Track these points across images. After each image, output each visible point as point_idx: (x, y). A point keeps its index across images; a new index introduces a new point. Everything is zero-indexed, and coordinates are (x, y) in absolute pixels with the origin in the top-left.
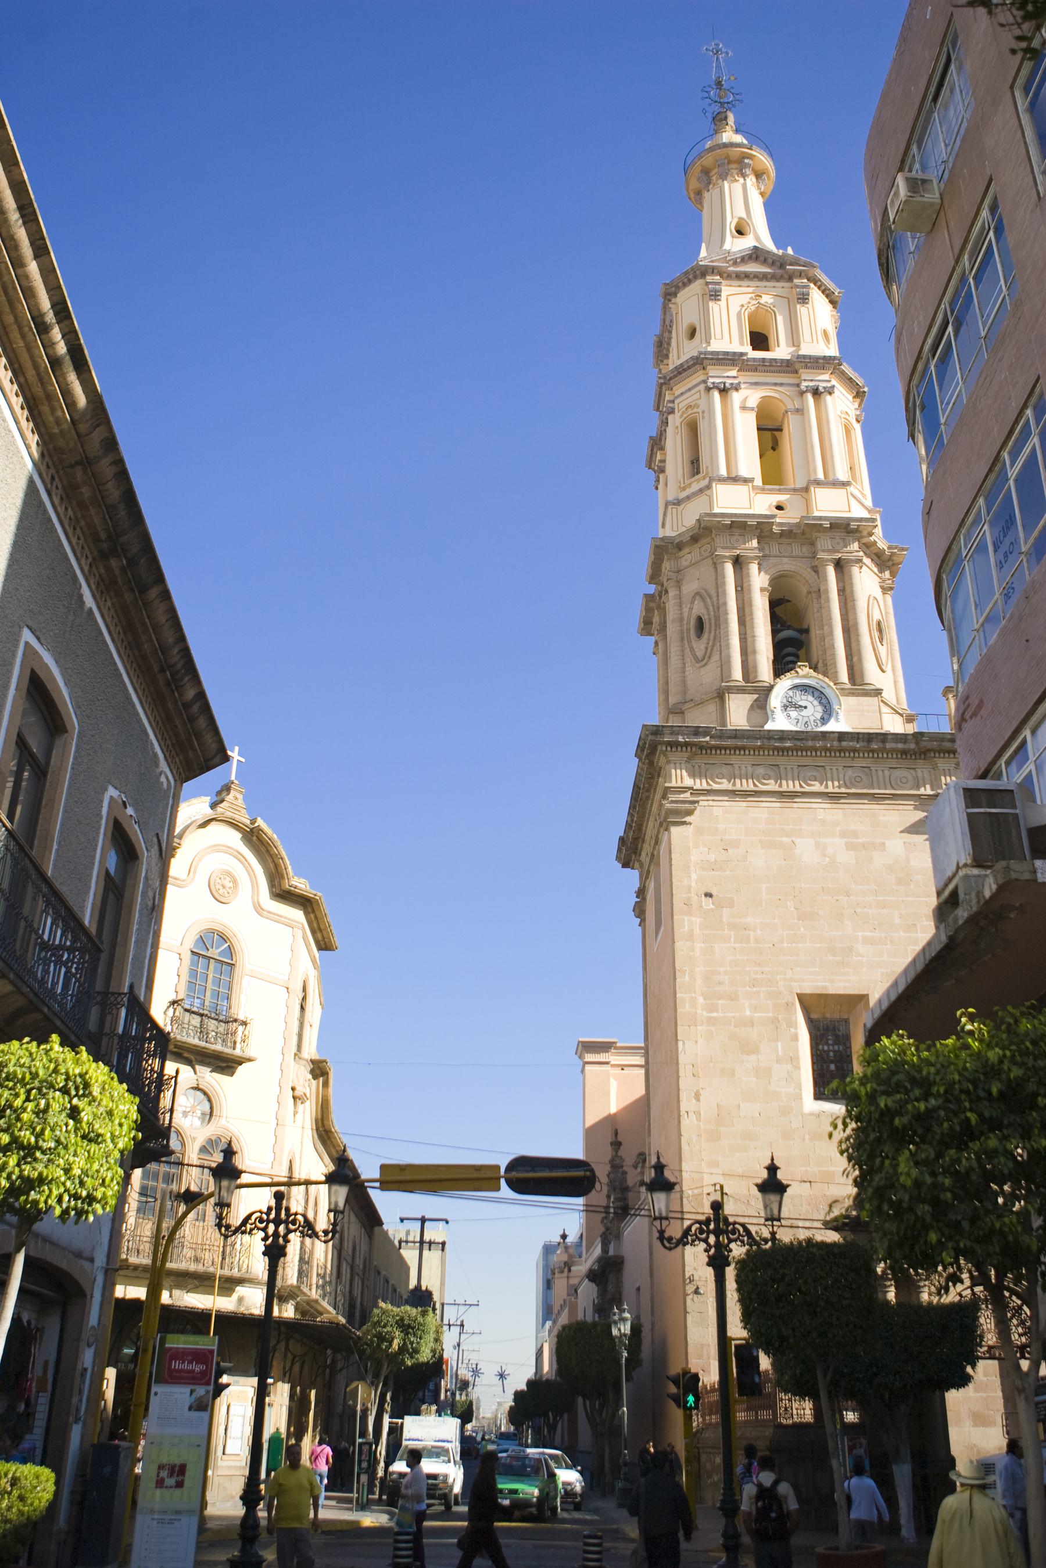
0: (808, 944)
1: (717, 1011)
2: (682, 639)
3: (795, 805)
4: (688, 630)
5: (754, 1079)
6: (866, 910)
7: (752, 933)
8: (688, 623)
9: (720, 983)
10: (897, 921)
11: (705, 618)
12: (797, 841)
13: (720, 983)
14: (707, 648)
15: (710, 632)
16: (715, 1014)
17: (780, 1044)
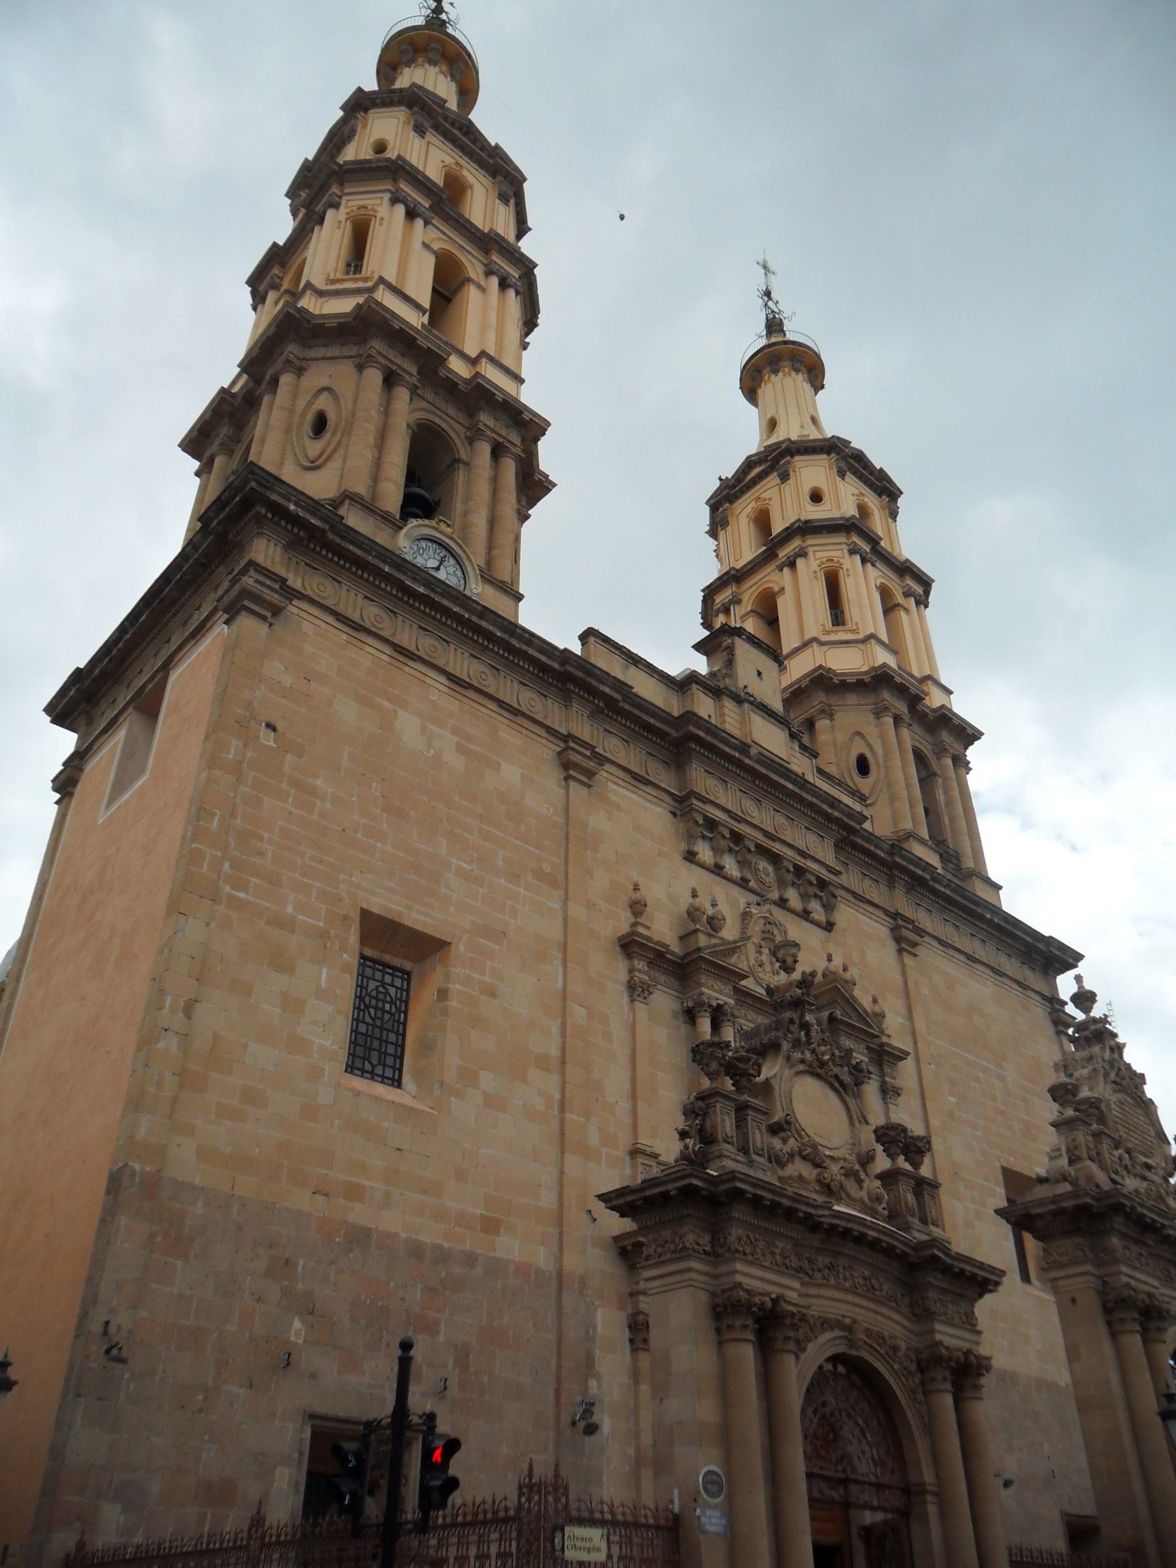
0: (388, 848)
1: (247, 894)
2: (288, 432)
3: (407, 669)
4: (300, 425)
5: (278, 1011)
6: (466, 834)
7: (318, 802)
8: (303, 415)
9: (260, 853)
10: (500, 863)
11: (331, 416)
12: (400, 712)
13: (260, 853)
15: (333, 435)
16: (242, 895)
17: (325, 971)
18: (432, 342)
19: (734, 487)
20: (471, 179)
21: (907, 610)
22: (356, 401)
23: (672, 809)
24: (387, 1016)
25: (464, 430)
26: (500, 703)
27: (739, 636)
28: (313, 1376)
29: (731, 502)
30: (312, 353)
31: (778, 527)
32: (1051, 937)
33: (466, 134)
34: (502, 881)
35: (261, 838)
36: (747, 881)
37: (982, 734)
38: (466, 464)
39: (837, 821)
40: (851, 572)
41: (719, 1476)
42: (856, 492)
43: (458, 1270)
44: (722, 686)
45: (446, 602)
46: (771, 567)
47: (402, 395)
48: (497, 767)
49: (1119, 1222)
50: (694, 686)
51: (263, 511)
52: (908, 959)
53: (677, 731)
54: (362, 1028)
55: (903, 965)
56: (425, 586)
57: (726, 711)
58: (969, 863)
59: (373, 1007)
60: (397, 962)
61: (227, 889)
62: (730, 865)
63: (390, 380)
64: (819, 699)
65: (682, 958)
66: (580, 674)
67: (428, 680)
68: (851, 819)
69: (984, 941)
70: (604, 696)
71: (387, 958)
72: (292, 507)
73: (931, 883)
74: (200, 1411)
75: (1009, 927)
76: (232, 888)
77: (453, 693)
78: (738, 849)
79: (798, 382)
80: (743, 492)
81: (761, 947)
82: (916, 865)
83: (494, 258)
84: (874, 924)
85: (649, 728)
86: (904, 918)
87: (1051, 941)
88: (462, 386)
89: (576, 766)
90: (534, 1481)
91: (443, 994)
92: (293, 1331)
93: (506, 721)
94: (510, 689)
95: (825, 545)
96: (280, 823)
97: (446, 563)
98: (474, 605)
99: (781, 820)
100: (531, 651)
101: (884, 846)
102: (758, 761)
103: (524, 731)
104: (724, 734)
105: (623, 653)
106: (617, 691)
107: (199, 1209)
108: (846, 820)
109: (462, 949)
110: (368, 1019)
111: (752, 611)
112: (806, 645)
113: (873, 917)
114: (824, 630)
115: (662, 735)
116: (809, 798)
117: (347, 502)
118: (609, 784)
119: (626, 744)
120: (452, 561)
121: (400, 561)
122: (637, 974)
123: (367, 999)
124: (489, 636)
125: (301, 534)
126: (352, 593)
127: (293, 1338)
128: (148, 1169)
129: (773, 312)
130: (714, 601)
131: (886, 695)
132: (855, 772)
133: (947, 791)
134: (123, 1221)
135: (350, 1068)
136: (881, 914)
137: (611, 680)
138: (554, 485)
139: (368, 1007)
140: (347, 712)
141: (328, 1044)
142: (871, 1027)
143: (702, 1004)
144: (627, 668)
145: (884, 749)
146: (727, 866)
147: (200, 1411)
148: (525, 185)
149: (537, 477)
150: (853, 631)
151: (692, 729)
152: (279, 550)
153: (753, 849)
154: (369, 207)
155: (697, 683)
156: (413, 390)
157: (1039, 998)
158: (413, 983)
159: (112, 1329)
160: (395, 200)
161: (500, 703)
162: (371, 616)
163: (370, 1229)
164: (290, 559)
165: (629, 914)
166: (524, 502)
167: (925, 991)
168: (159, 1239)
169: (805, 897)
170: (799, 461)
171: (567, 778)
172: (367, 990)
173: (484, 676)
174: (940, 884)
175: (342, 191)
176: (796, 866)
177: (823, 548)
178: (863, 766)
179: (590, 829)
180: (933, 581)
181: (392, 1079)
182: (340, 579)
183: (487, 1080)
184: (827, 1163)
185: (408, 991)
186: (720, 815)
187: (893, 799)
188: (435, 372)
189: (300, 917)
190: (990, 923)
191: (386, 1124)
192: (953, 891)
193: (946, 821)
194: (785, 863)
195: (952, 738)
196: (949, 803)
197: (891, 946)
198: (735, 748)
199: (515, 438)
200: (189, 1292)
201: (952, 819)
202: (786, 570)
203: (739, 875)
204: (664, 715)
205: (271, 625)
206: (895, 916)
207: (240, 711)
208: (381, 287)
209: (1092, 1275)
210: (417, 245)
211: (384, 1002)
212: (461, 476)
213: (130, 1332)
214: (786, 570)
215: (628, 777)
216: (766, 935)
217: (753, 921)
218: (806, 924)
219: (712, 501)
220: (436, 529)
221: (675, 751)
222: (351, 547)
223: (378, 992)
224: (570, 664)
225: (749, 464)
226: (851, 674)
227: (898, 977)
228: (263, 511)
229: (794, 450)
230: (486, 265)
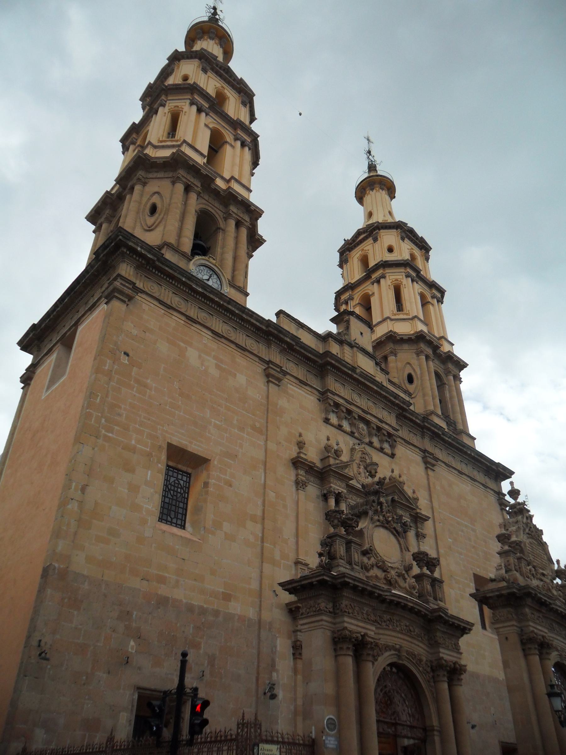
0: (181, 414)
1: (112, 433)
2: (138, 213)
5: (126, 491)
6: (219, 408)
7: (148, 391)
8: (145, 205)
10: (235, 422)
11: (159, 206)
12: (189, 348)
13: (120, 415)
14: (155, 223)
15: (160, 215)
16: (110, 435)
17: (149, 472)
18: (209, 172)
19: (351, 244)
20: (228, 94)
21: (433, 305)
22: (171, 199)
23: (318, 398)
24: (179, 495)
25: (222, 214)
26: (237, 345)
27: (352, 315)
28: (139, 668)
29: (350, 251)
30: (150, 176)
31: (372, 264)
32: (499, 463)
33: (227, 73)
34: (236, 431)
35: (120, 407)
36: (354, 433)
37: (468, 365)
38: (223, 230)
39: (397, 405)
40: (406, 286)
41: (334, 720)
42: (409, 248)
43: (211, 618)
44: (343, 339)
45: (212, 296)
46: (368, 283)
47: (193, 196)
48: (235, 376)
49: (529, 601)
50: (330, 339)
51: (125, 250)
52: (430, 472)
53: (321, 360)
54: (167, 500)
55: (428, 475)
56: (202, 288)
57: (345, 351)
58: (460, 427)
59: (172, 490)
60: (184, 468)
61: (103, 432)
62: (346, 425)
63: (188, 189)
64: (390, 346)
65: (322, 469)
66: (276, 332)
67: (202, 333)
68: (404, 405)
69: (467, 464)
70: (287, 343)
71: (180, 466)
72: (139, 249)
73: (442, 436)
74: (84, 684)
75: (479, 458)
76: (106, 431)
77: (214, 340)
78: (350, 417)
79: (384, 194)
80: (355, 247)
81: (360, 465)
82: (435, 427)
83: (239, 132)
84: (414, 455)
85: (308, 359)
86: (428, 452)
87: (499, 465)
88: (222, 193)
89: (273, 376)
90: (245, 721)
91: (206, 484)
92: (130, 647)
93: (239, 354)
94: (241, 338)
95: (395, 272)
96: (129, 400)
97: (212, 278)
98: (226, 298)
99: (370, 404)
100: (252, 320)
101: (420, 417)
102: (360, 376)
103: (248, 359)
104: (344, 362)
105: (296, 322)
106: (293, 340)
107: (86, 586)
108: (401, 404)
109: (216, 463)
110: (169, 496)
111: (359, 304)
112: (384, 320)
113: (414, 452)
114: (393, 313)
115: (314, 362)
116: (384, 393)
117: (166, 247)
118: (288, 385)
119: (297, 366)
120: (215, 277)
121: (190, 276)
122: (300, 476)
123: (169, 486)
124: (232, 313)
125: (143, 262)
126: (167, 290)
127: (130, 650)
128: (62, 566)
129: (371, 161)
130: (341, 298)
131: (422, 346)
132: (406, 381)
133: (450, 392)
134: (49, 591)
135: (161, 520)
136: (417, 450)
137: (290, 335)
138: (265, 241)
139: (170, 490)
140: (163, 347)
141: (150, 508)
142: (412, 504)
143: (330, 492)
144: (298, 329)
145: (420, 371)
146: (344, 426)
147: (84, 684)
148: (254, 98)
149: (257, 237)
150: (407, 314)
151: (329, 359)
152: (132, 270)
153: (357, 418)
154: (180, 106)
155: (332, 338)
156: (199, 194)
157: (492, 492)
158: (192, 479)
159: (42, 644)
160: (192, 104)
161: (237, 345)
162: (176, 303)
163: (168, 598)
164: (137, 273)
165: (297, 448)
166: (250, 249)
167: (438, 488)
168: (66, 600)
169: (381, 441)
170: (383, 232)
171: (268, 382)
172: (169, 482)
173: (229, 332)
174: (447, 437)
175: (167, 98)
176: (377, 426)
177: (393, 274)
178: (410, 379)
179: (278, 407)
180: (446, 291)
181: (181, 525)
182: (161, 284)
183: (226, 527)
184: (389, 570)
185: (189, 483)
186: (341, 401)
187: (424, 395)
188: (209, 185)
189: (138, 446)
190: (470, 455)
191: (177, 547)
192: (453, 440)
193: (450, 406)
194: (372, 425)
195: (453, 367)
196: (451, 397)
197: (422, 466)
198: (349, 369)
199: (247, 218)
200: (80, 627)
201: (453, 406)
202: (375, 284)
203: (350, 430)
204: (315, 352)
205: (127, 305)
206: (424, 451)
207: (111, 346)
208: (184, 145)
209: (516, 626)
210: (202, 125)
211: (178, 488)
212: (220, 236)
213: (51, 645)
214: (375, 284)
215: (297, 382)
216: (363, 459)
217: (356, 452)
218: (381, 454)
219: (341, 250)
220: (208, 261)
221: (320, 370)
222: (167, 269)
223: (175, 483)
224: (270, 327)
225: (359, 233)
226: (406, 335)
227: (426, 482)
228: (125, 250)
229: (380, 227)
230: (234, 135)
